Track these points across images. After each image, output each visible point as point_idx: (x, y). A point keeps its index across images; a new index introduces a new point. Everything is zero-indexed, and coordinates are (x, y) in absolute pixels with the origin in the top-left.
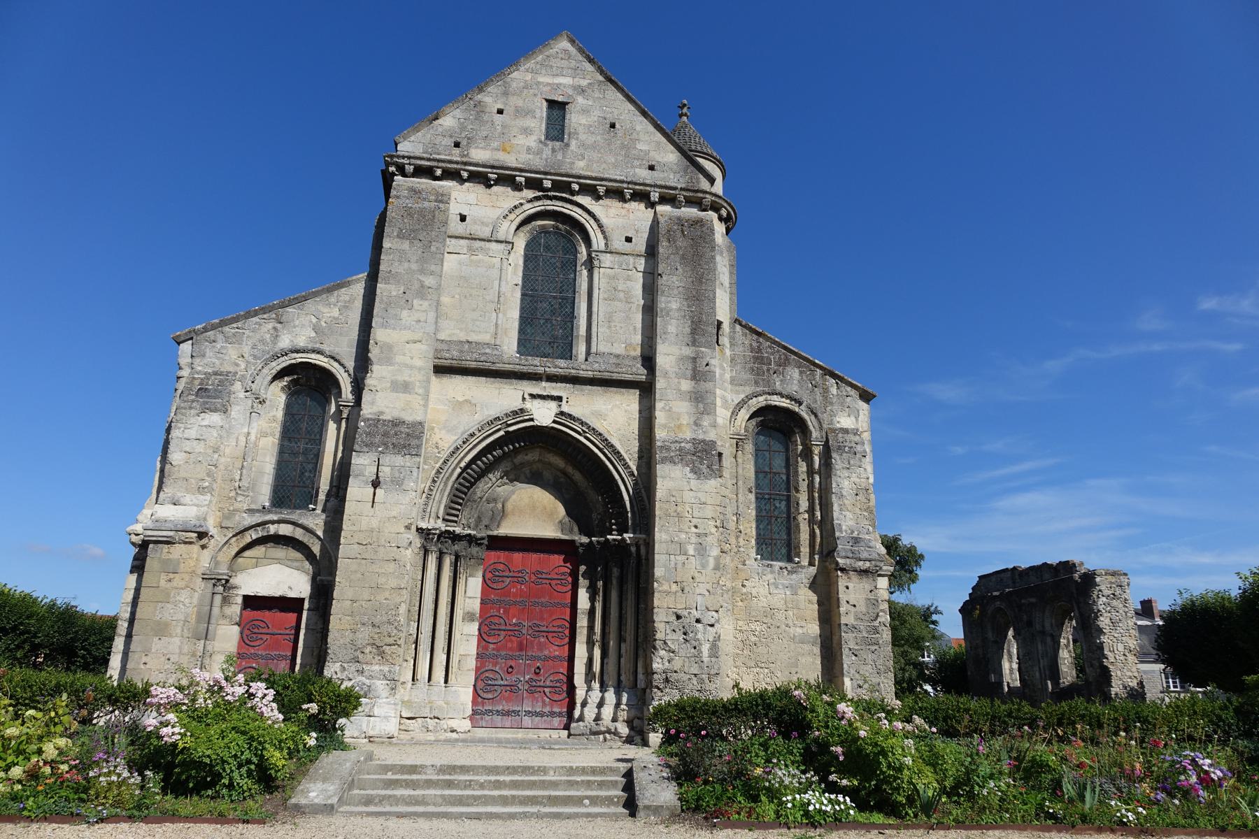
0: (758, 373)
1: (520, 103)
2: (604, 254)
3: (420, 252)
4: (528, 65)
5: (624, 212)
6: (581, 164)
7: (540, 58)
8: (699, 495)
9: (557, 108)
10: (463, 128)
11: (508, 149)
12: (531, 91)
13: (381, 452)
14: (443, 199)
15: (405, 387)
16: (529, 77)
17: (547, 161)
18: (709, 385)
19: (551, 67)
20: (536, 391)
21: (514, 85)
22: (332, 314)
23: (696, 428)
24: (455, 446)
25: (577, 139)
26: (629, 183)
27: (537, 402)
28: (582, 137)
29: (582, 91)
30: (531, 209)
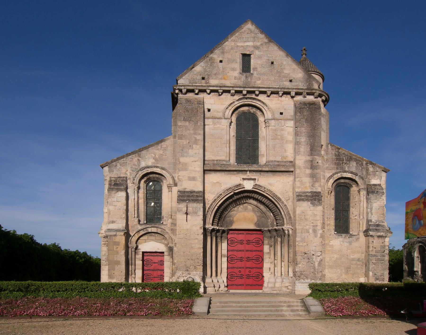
0: (338, 164)
1: (230, 57)
2: (271, 121)
3: (193, 126)
4: (232, 38)
5: (279, 102)
6: (259, 82)
7: (237, 34)
8: (314, 212)
9: (246, 57)
10: (205, 71)
11: (226, 78)
12: (235, 50)
13: (187, 202)
16: (233, 44)
17: (244, 82)
18: (318, 171)
19: (243, 38)
20: (245, 177)
21: (226, 48)
22: (160, 153)
23: (312, 187)
24: (214, 199)
25: (257, 71)
26: (281, 88)
27: (245, 182)
28: (259, 69)
30: (238, 104)
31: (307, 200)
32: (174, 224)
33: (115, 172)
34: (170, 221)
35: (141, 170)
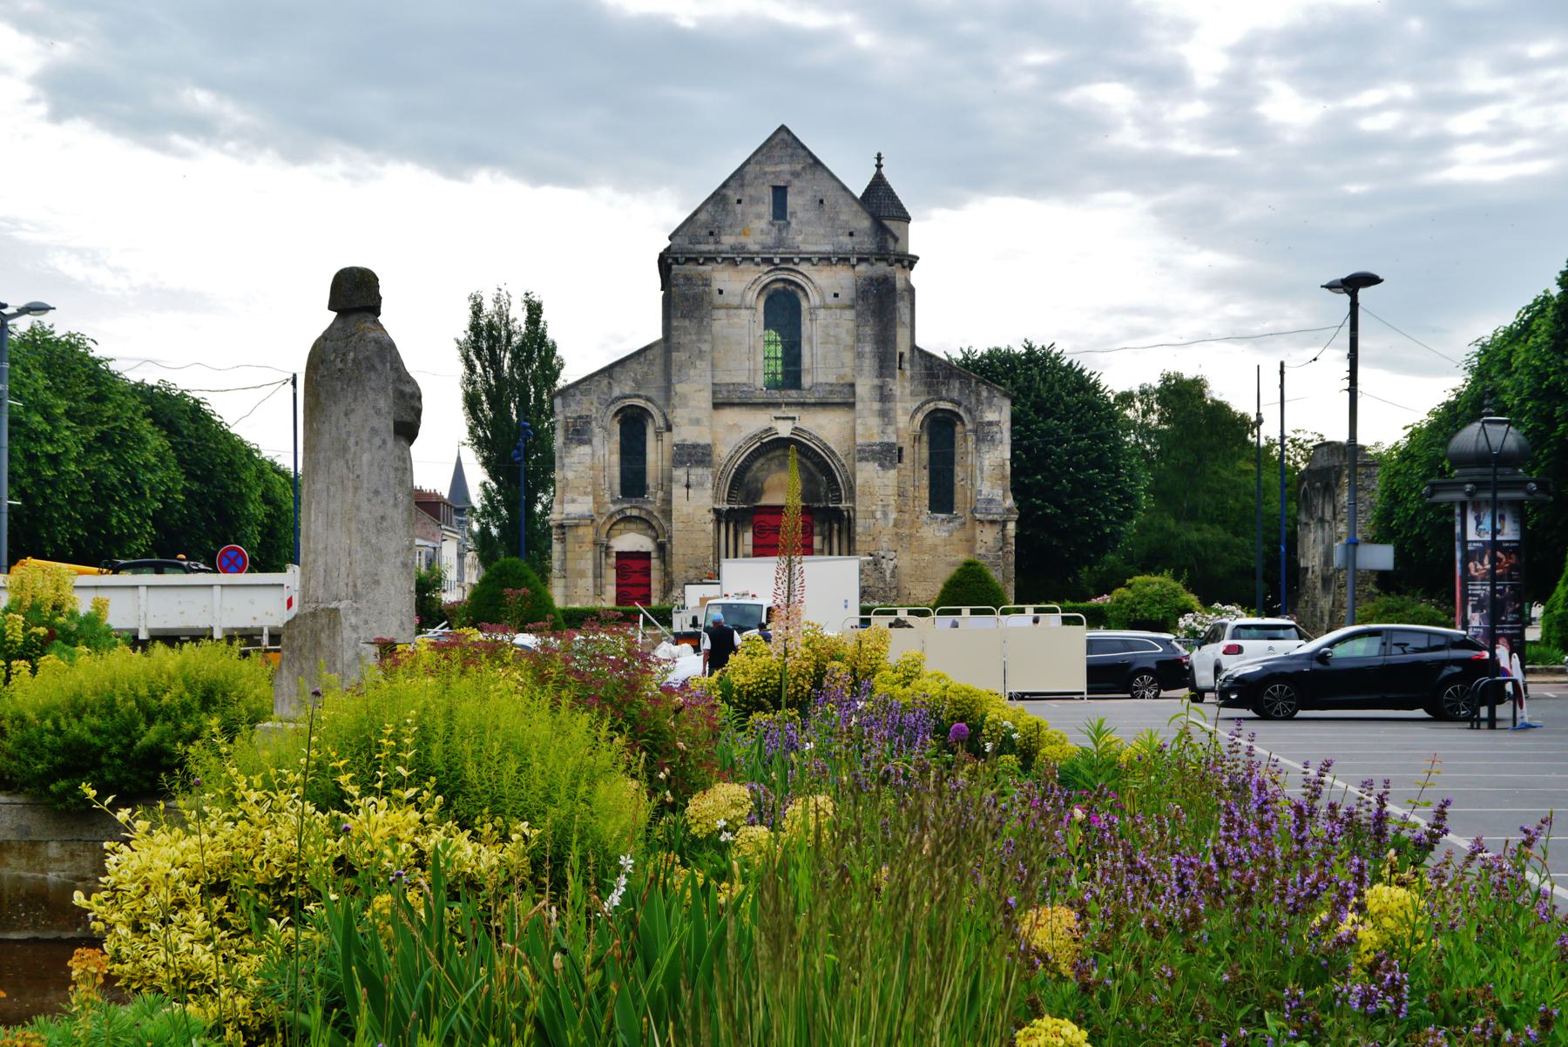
0: (929, 385)
9: (780, 193)
14: (707, 283)
15: (697, 422)
20: (779, 414)
27: (779, 422)
28: (800, 215)
29: (796, 175)
30: (766, 279)
31: (874, 459)
32: (668, 501)
33: (574, 406)
34: (660, 494)
35: (613, 402)
